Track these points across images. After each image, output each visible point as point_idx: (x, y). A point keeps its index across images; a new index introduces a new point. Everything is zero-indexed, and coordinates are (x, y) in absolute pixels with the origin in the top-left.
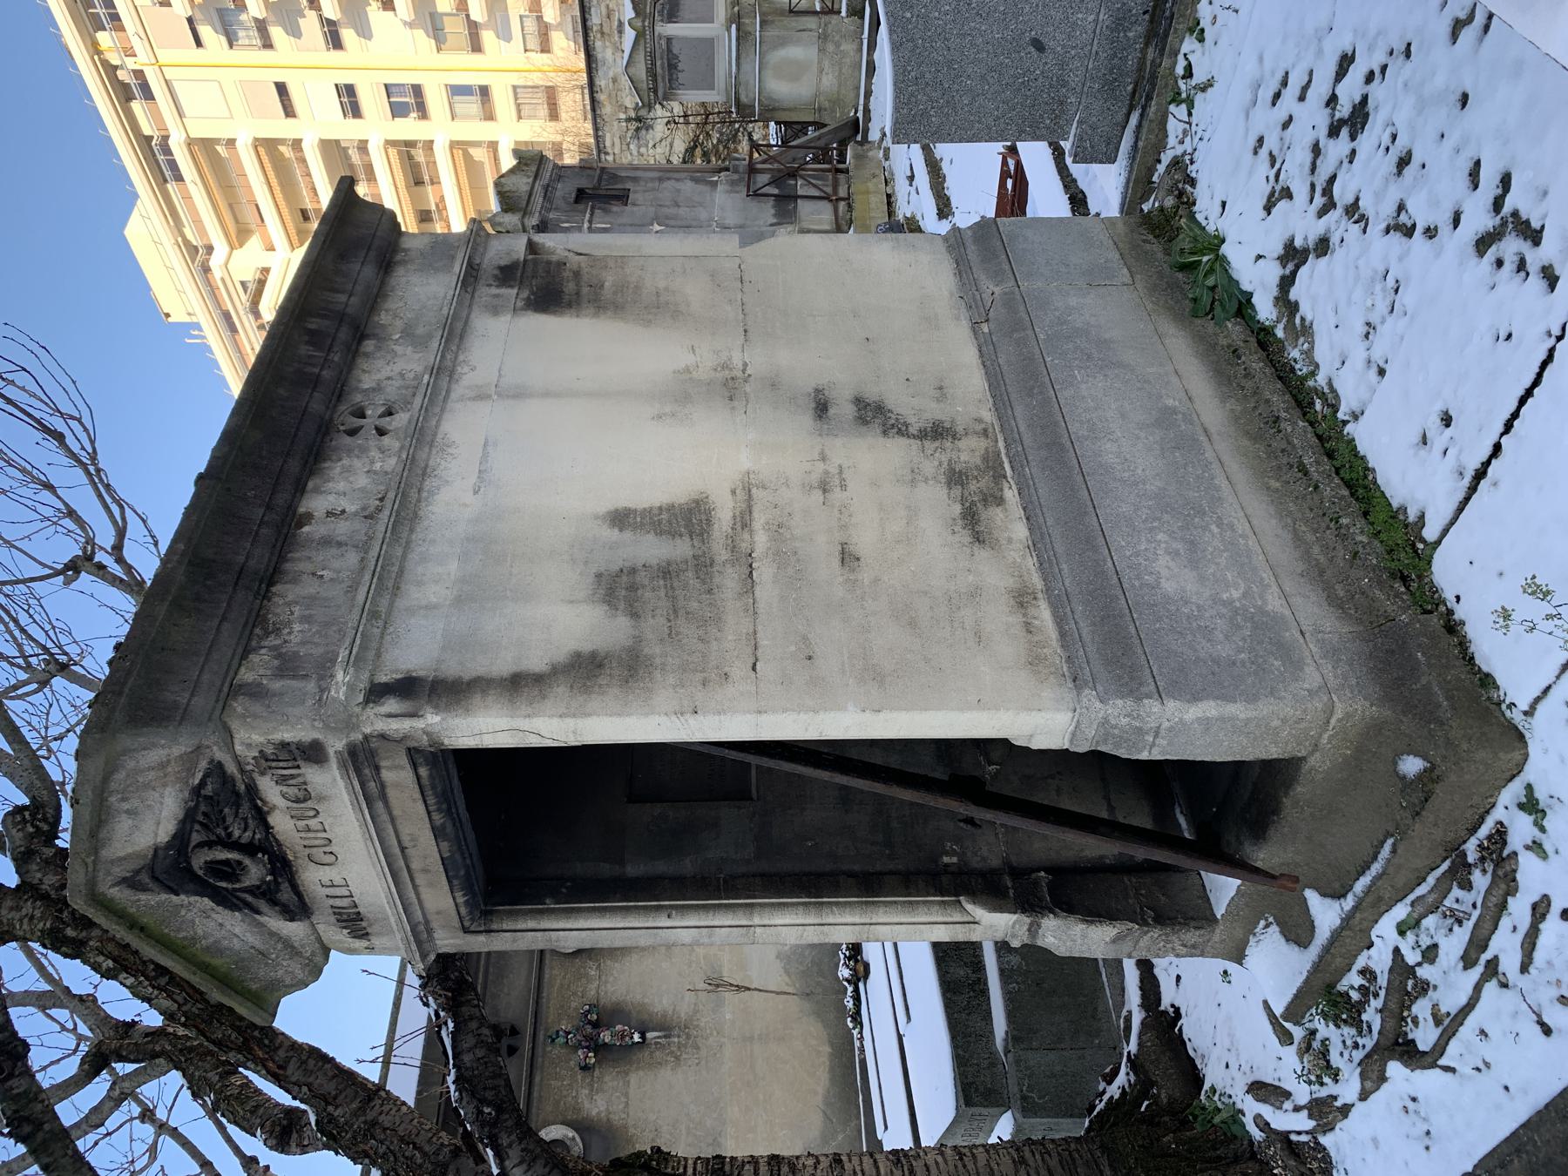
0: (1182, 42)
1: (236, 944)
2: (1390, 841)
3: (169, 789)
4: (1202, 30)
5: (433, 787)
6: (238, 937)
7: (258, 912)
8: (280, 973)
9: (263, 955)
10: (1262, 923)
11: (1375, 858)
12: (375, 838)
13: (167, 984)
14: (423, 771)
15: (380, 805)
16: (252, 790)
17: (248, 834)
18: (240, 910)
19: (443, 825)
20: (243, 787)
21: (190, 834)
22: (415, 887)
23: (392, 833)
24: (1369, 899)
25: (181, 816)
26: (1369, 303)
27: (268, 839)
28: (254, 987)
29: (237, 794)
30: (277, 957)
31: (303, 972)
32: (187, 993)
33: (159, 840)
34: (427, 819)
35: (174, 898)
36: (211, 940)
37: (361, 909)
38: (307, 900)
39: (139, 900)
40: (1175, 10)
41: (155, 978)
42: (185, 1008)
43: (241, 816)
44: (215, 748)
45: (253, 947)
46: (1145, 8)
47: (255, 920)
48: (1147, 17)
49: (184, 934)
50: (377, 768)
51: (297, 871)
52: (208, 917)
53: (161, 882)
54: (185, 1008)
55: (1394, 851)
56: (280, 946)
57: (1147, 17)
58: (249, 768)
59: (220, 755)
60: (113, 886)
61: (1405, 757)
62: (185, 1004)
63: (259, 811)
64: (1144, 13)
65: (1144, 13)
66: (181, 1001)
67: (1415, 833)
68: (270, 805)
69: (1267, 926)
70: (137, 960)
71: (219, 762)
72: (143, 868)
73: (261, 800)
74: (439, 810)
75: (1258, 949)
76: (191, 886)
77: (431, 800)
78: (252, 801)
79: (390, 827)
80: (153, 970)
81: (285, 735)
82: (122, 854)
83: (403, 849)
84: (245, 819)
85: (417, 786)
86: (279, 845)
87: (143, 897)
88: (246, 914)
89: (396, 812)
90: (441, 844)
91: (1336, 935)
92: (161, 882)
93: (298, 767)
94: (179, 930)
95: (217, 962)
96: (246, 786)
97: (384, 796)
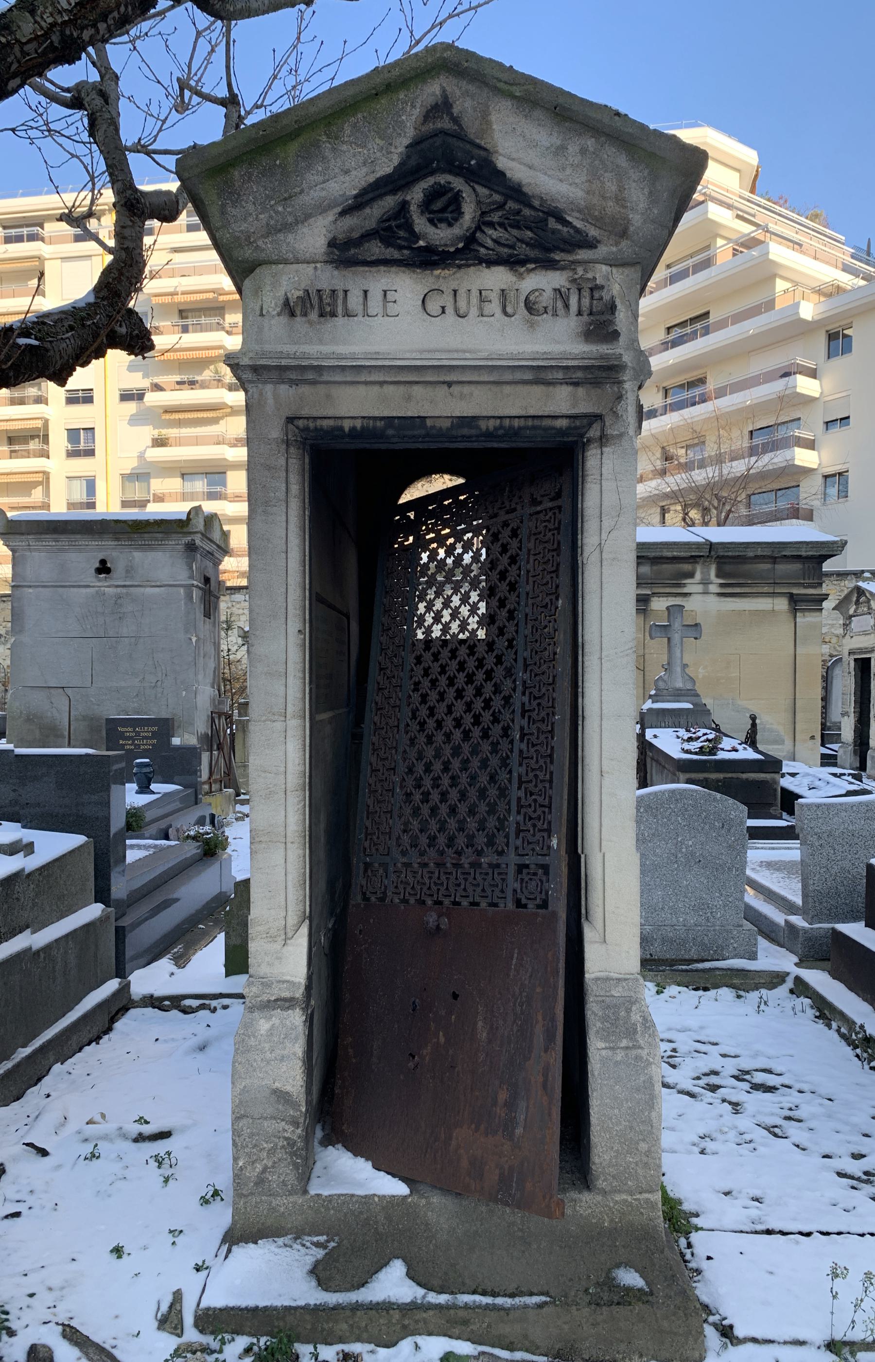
0: (650, 981)
1: (312, 177)
2: (543, 1298)
3: (580, 194)
4: (662, 992)
5: (534, 428)
6: (324, 182)
7: (343, 213)
8: (251, 208)
9: (285, 199)
10: (322, 1239)
11: (512, 1296)
12: (490, 363)
13: (52, 42)
14: (562, 423)
15: (528, 376)
16: (550, 265)
17: (489, 243)
18: (356, 197)
19: (478, 427)
20: (557, 258)
21: (489, 188)
22: (382, 383)
23: (482, 379)
24: (461, 1313)
25: (525, 189)
26: (726, 1129)
27: (475, 259)
28: (236, 173)
29: (549, 250)
30: (277, 212)
31: (241, 231)
32: (35, 58)
33: (500, 158)
34: (496, 415)
35: (406, 141)
36: (328, 153)
37: (340, 321)
38: (362, 269)
39: (413, 106)
40: (667, 972)
41: (62, 33)
42: (17, 48)
43: (519, 244)
44: (614, 249)
45: (302, 192)
46: (654, 954)
47: (339, 205)
48: (649, 956)
49: (348, 132)
50: (576, 384)
51: (414, 272)
52: (364, 164)
53: (431, 137)
54: (17, 48)
55: (540, 1306)
56: (290, 219)
57: (649, 956)
58: (580, 271)
59: (602, 250)
60: (444, 91)
61: (632, 1270)
62: (22, 51)
63: (523, 262)
64: (651, 955)
65: (651, 955)
66: (26, 48)
67: (576, 1313)
68: (525, 274)
69: (317, 1245)
70: (86, 22)
71: (596, 247)
72: (460, 126)
73: (533, 269)
74: (501, 427)
75: (277, 1250)
76: (413, 162)
77: (516, 423)
78: (535, 261)
79: (492, 379)
80: (72, 34)
81: (622, 314)
82: (493, 118)
83: (449, 384)
84: (512, 247)
85: (546, 414)
86: (459, 267)
87: (417, 112)
88: (347, 200)
89: (507, 389)
90: (451, 420)
91: (386, 1307)
92: (431, 137)
93: (580, 313)
94: (354, 126)
95: (293, 147)
96: (556, 261)
97: (537, 382)
